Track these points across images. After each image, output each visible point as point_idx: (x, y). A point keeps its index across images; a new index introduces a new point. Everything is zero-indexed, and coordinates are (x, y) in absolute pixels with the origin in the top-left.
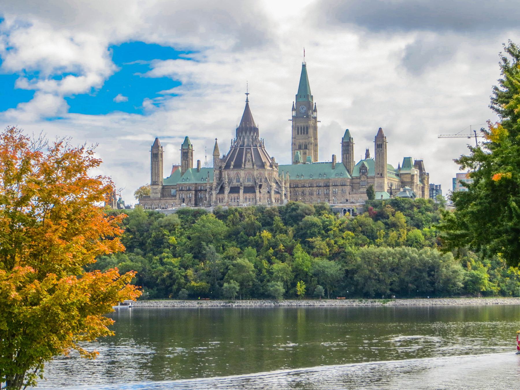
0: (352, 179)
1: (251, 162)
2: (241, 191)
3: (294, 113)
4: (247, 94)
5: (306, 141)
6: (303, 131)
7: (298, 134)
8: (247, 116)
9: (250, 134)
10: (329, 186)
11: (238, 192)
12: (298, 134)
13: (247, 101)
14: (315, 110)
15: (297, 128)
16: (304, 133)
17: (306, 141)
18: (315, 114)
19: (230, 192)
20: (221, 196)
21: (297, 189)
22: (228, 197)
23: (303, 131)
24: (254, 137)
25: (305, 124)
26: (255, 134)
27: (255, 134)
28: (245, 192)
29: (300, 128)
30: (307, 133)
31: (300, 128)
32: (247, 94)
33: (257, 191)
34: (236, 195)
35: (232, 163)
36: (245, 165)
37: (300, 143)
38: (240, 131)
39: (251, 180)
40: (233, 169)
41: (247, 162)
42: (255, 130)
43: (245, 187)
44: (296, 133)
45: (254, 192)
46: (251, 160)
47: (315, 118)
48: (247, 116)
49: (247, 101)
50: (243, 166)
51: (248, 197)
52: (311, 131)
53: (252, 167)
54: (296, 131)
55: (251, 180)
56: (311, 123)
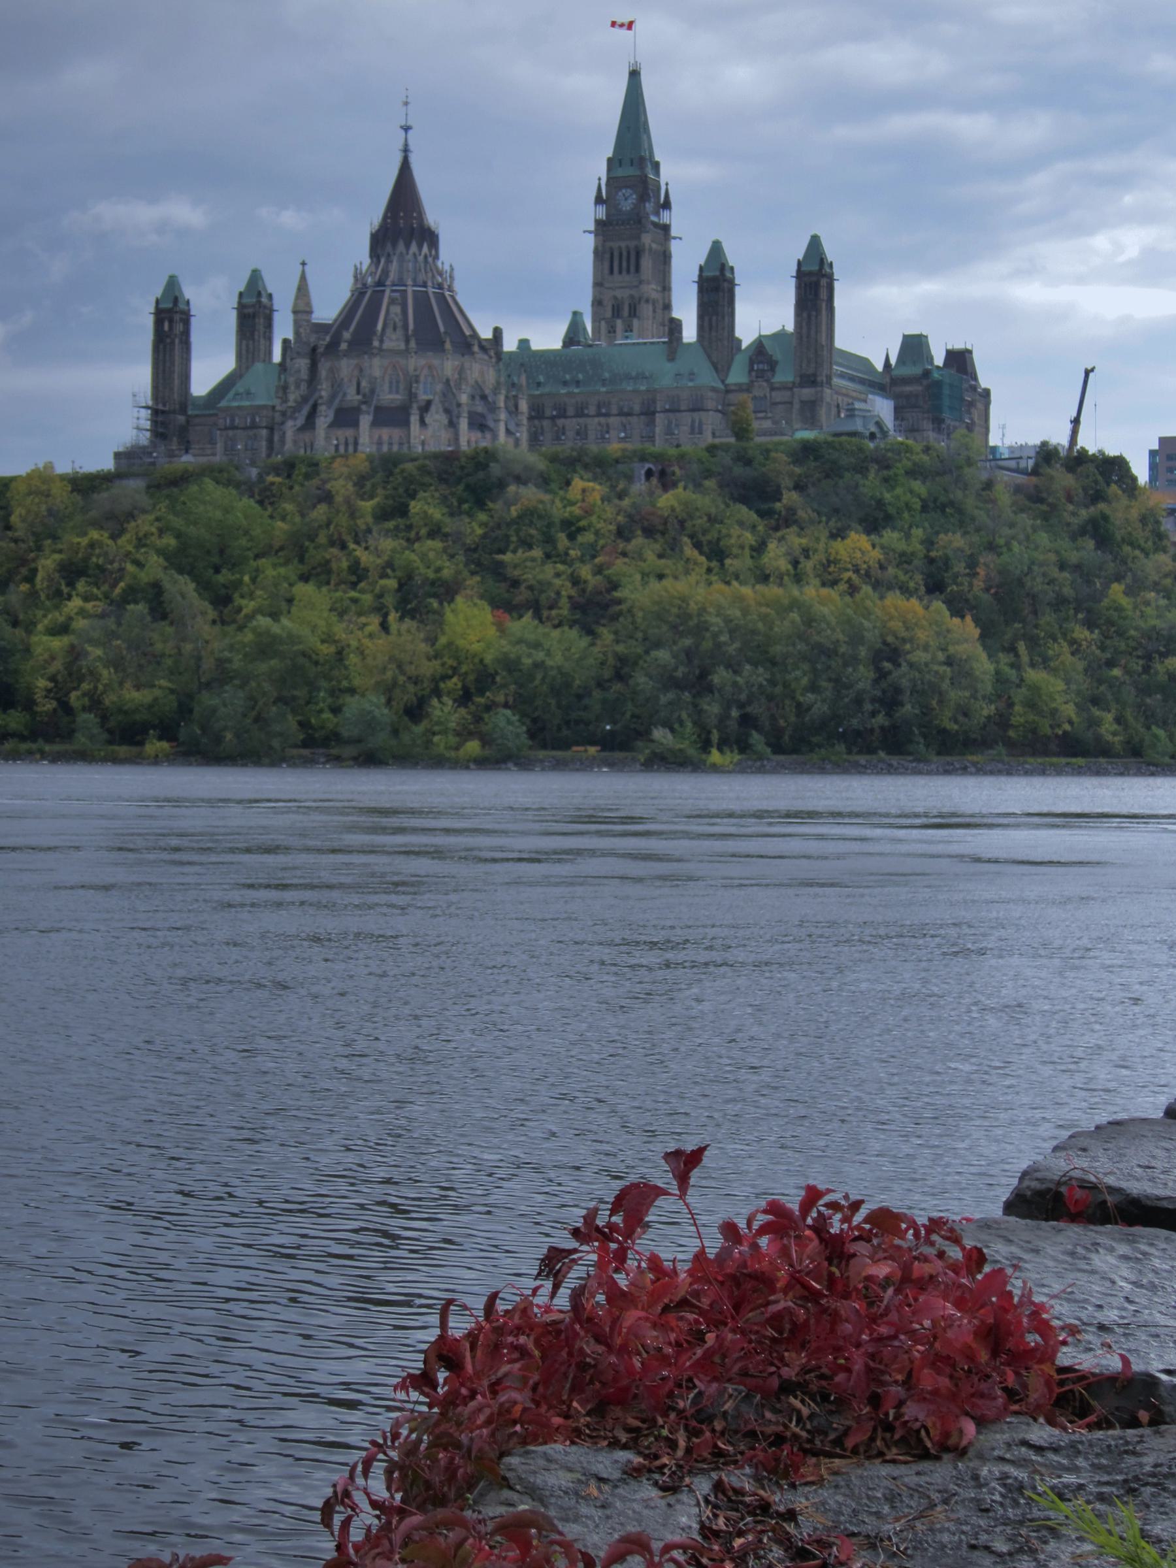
0: (728, 391)
1: (400, 333)
2: (365, 421)
3: (602, 212)
4: (406, 129)
5: (633, 292)
6: (624, 264)
7: (611, 272)
8: (404, 194)
9: (408, 246)
10: (654, 413)
11: (355, 424)
12: (611, 272)
13: (406, 150)
14: (667, 205)
15: (607, 256)
16: (628, 271)
17: (633, 292)
18: (665, 217)
19: (332, 425)
20: (307, 436)
21: (560, 422)
22: (328, 438)
23: (624, 264)
24: (421, 258)
25: (632, 244)
26: (425, 249)
27: (425, 249)
28: (376, 423)
29: (616, 254)
30: (637, 269)
31: (616, 254)
32: (406, 129)
33: (414, 419)
34: (349, 433)
35: (347, 335)
36: (381, 341)
37: (615, 298)
38: (381, 241)
39: (402, 387)
40: (346, 354)
41: (389, 331)
42: (429, 237)
43: (378, 409)
44: (606, 271)
45: (406, 423)
46: (399, 324)
47: (666, 228)
48: (404, 194)
49: (406, 150)
50: (376, 343)
51: (385, 438)
52: (647, 263)
53: (402, 346)
54: (606, 265)
55: (402, 387)
56: (647, 239)
